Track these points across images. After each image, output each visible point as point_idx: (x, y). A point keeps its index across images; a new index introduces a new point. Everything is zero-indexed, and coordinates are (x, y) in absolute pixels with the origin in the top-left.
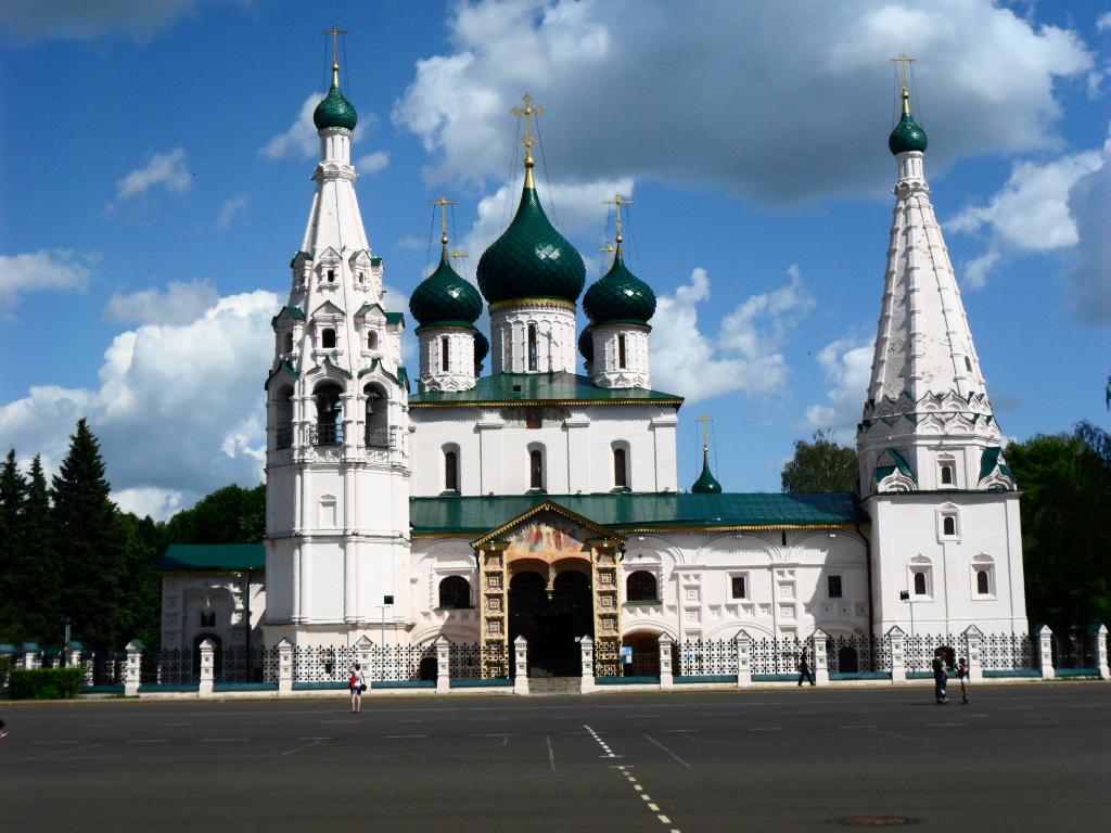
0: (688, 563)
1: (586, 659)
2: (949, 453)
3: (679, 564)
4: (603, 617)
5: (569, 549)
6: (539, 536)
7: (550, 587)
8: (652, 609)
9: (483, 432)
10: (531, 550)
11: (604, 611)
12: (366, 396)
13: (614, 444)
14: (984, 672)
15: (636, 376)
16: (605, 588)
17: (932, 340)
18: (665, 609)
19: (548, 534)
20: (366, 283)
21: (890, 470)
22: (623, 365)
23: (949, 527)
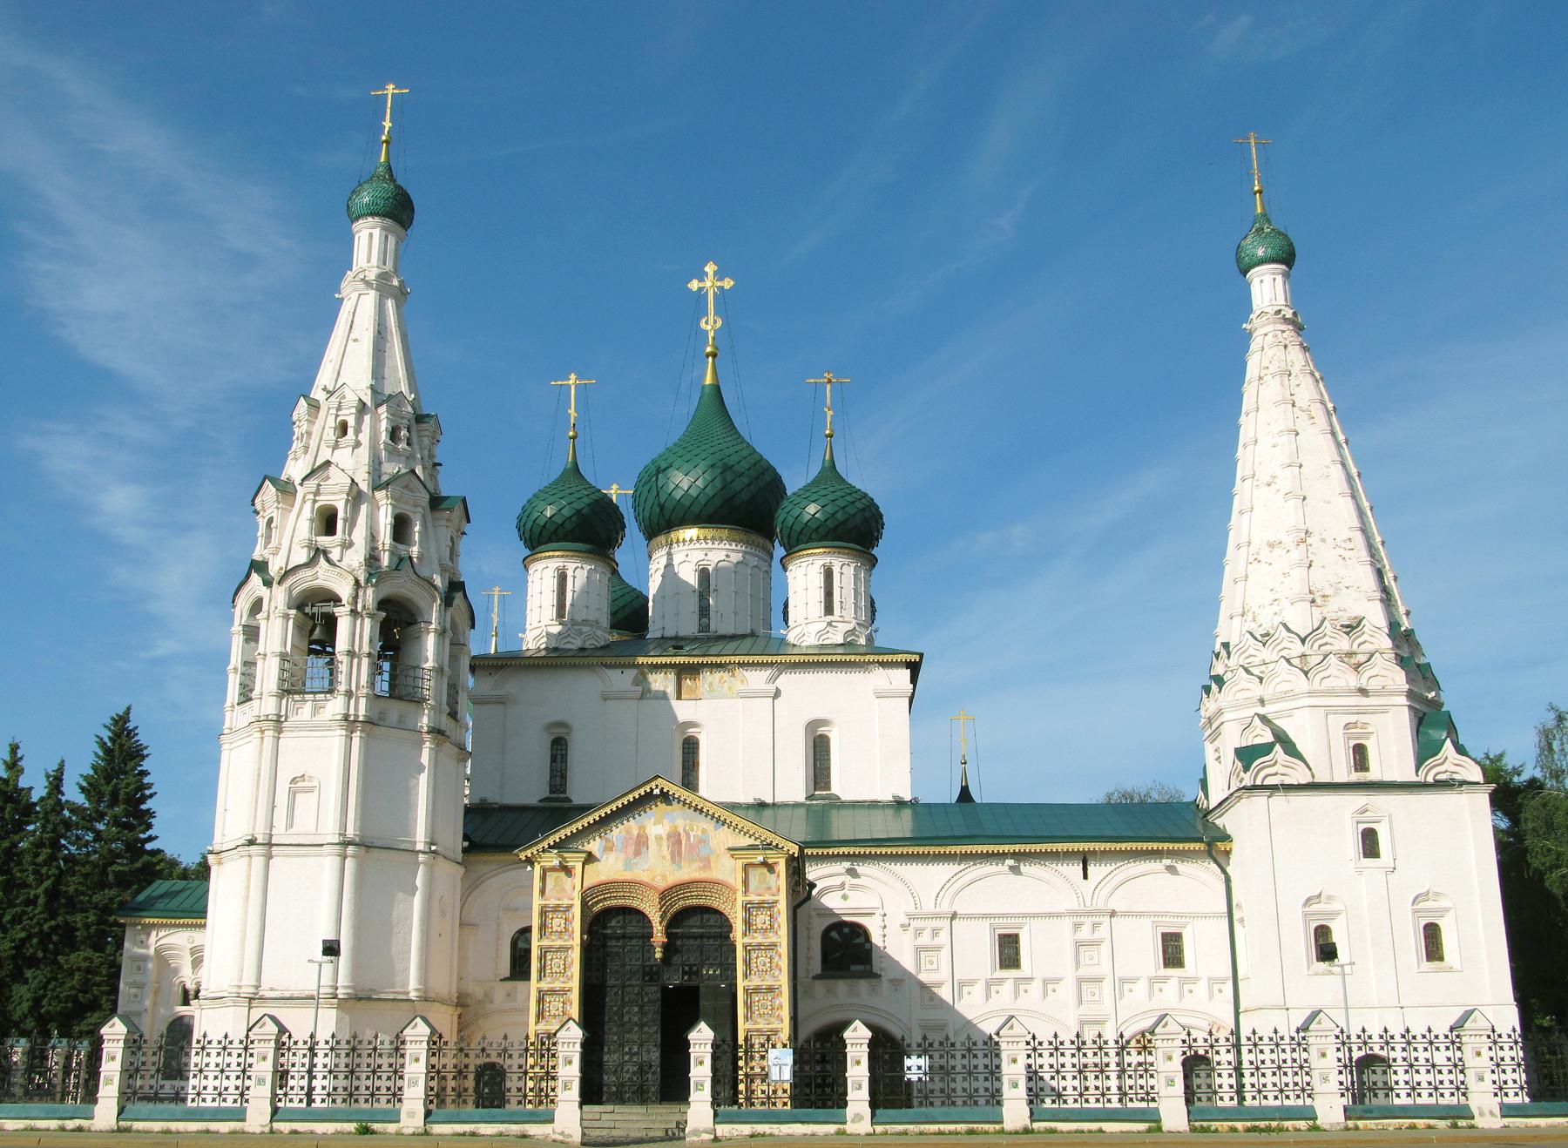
0: (928, 906)
1: (701, 1072)
2: (1363, 718)
3: (911, 909)
4: (757, 990)
5: (695, 865)
6: (641, 843)
7: (659, 936)
8: (863, 985)
9: (608, 702)
10: (628, 866)
11: (755, 981)
12: (384, 614)
13: (813, 725)
14: (1502, 1106)
15: (850, 627)
16: (758, 938)
17: (1323, 540)
18: (885, 984)
19: (659, 838)
20: (402, 446)
21: (1266, 749)
22: (829, 610)
23: (1370, 844)
